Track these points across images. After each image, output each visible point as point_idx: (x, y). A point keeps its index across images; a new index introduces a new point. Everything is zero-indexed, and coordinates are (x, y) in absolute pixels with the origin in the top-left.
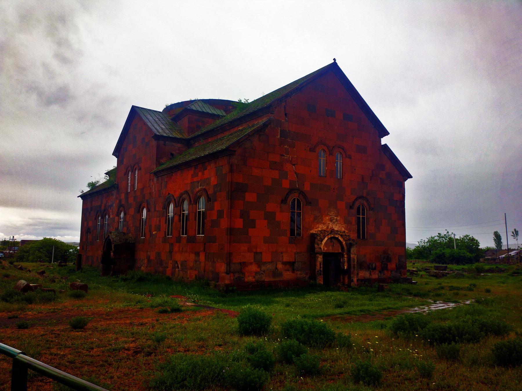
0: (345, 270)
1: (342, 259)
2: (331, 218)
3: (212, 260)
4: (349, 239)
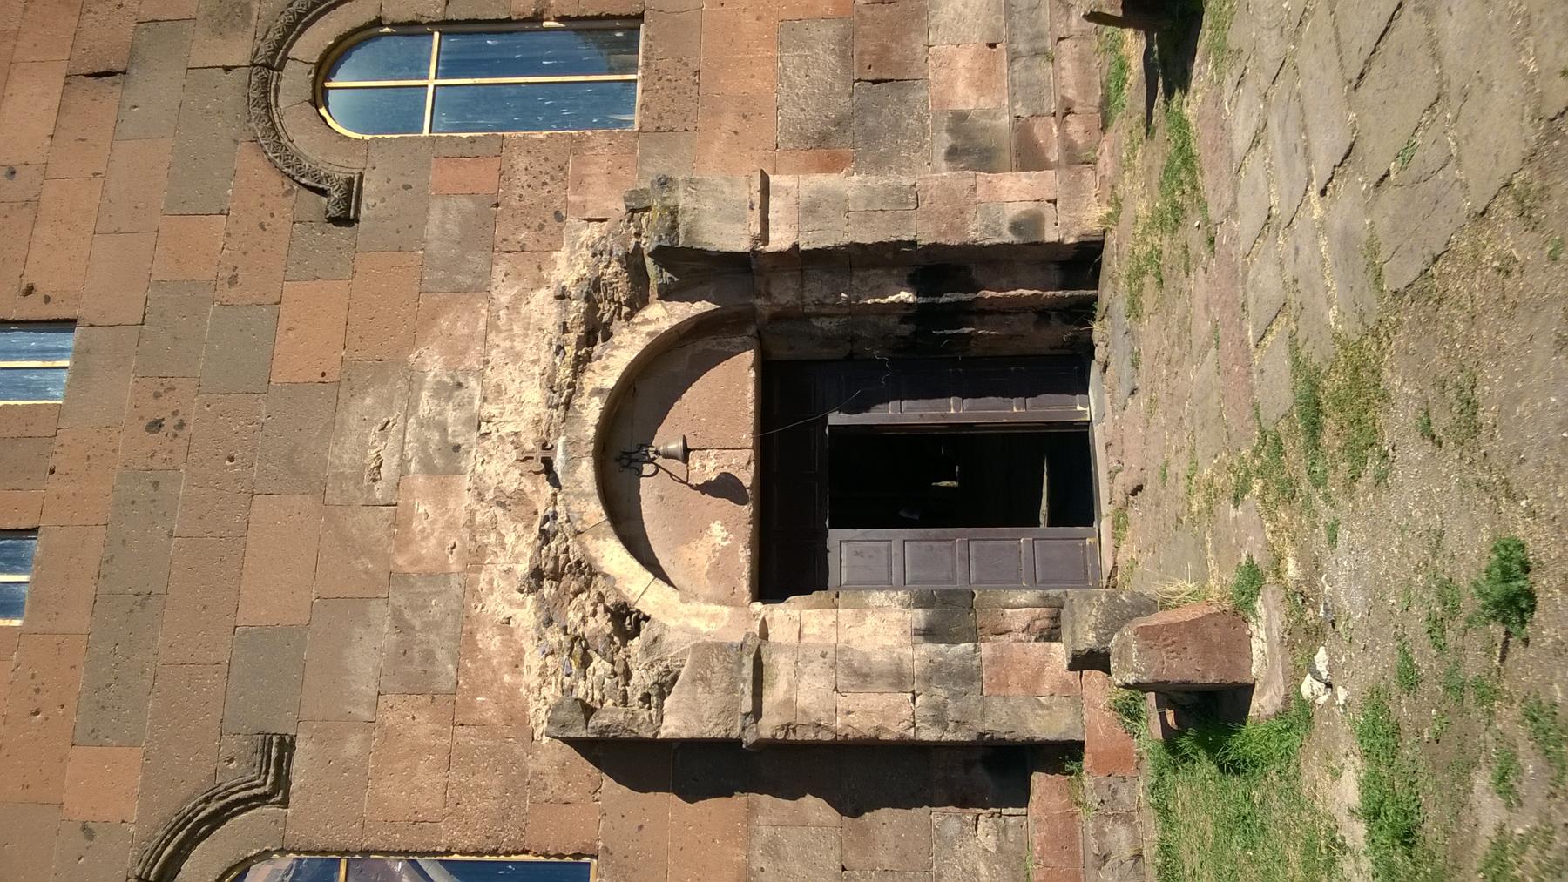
1: (816, 323)
2: (428, 468)
4: (633, 263)
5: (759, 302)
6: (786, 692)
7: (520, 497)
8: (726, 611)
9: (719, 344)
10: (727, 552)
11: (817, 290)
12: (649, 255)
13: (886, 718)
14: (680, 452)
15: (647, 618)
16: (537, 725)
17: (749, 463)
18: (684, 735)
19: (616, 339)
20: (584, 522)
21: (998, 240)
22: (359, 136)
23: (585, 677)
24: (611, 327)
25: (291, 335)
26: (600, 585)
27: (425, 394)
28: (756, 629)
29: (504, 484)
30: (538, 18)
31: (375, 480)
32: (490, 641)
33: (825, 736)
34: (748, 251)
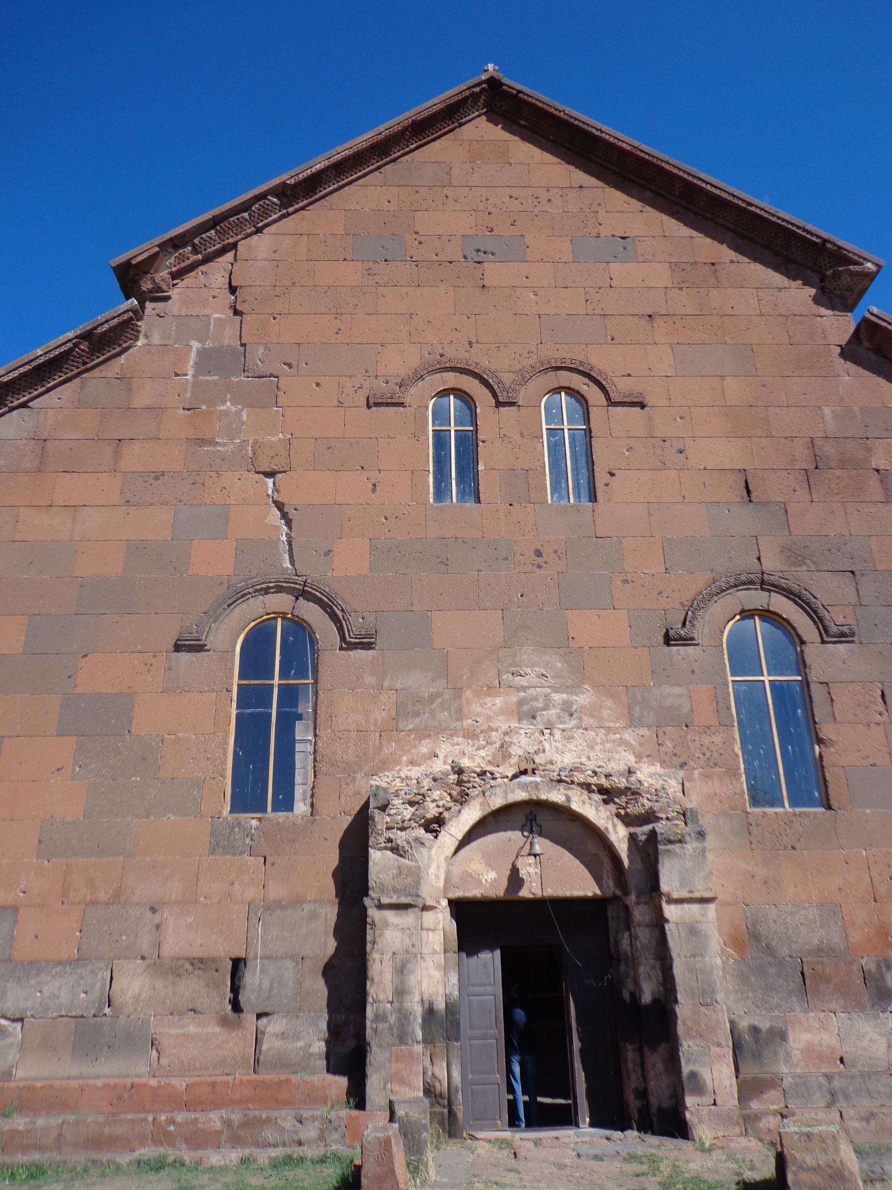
0: (647, 1006)
1: (626, 935)
2: (521, 703)
4: (649, 817)
5: (633, 897)
6: (393, 923)
7: (506, 756)
8: (441, 884)
9: (608, 872)
10: (479, 882)
11: (644, 936)
12: (654, 828)
13: (378, 984)
14: (534, 852)
15: (436, 837)
16: (380, 777)
17: (533, 894)
18: (371, 863)
19: (602, 808)
20: (490, 796)
21: (683, 1061)
22: (724, 640)
23: (403, 803)
24: (612, 804)
25: (596, 618)
26: (455, 808)
27: (565, 696)
28: (430, 902)
29: (514, 747)
30: (820, 741)
31: (513, 674)
32: (424, 748)
33: (369, 947)
34: (662, 890)
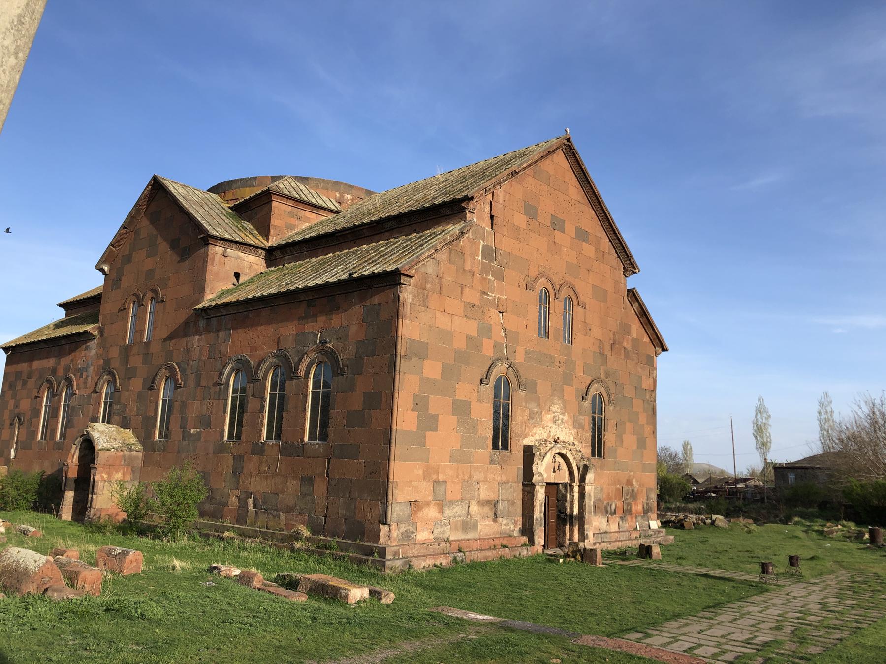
2: (554, 417)
3: (347, 494)
7: (550, 436)
